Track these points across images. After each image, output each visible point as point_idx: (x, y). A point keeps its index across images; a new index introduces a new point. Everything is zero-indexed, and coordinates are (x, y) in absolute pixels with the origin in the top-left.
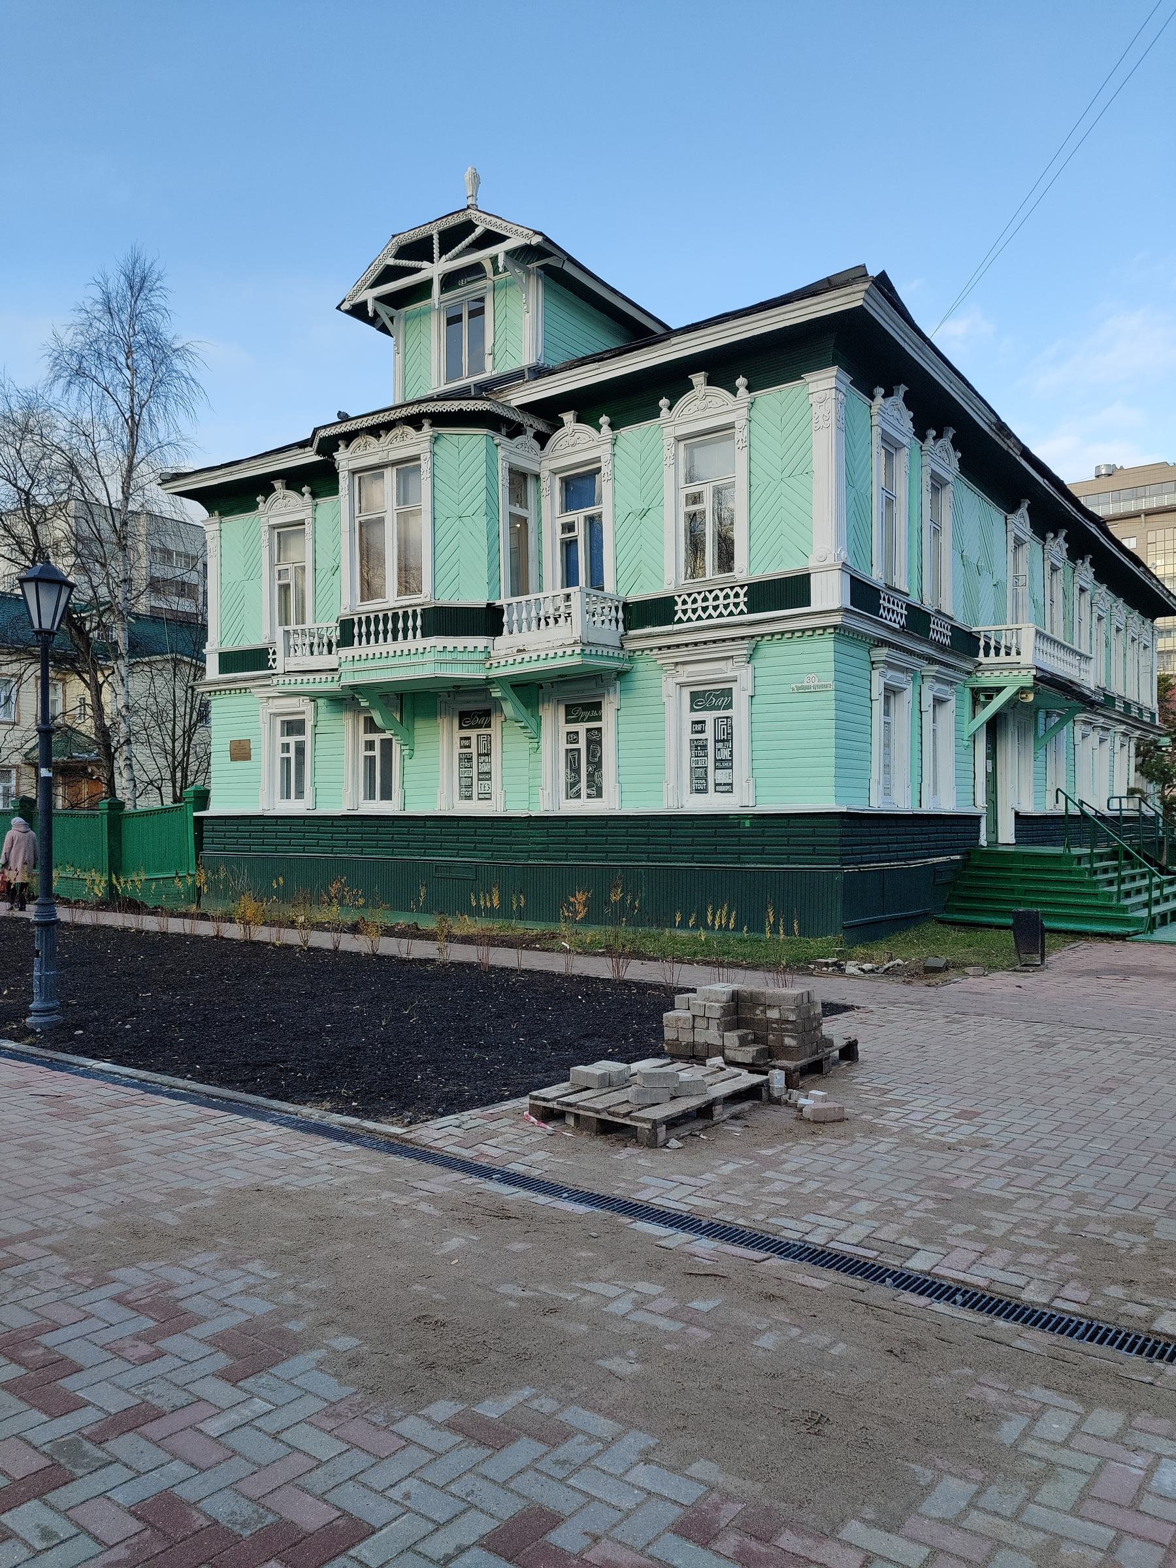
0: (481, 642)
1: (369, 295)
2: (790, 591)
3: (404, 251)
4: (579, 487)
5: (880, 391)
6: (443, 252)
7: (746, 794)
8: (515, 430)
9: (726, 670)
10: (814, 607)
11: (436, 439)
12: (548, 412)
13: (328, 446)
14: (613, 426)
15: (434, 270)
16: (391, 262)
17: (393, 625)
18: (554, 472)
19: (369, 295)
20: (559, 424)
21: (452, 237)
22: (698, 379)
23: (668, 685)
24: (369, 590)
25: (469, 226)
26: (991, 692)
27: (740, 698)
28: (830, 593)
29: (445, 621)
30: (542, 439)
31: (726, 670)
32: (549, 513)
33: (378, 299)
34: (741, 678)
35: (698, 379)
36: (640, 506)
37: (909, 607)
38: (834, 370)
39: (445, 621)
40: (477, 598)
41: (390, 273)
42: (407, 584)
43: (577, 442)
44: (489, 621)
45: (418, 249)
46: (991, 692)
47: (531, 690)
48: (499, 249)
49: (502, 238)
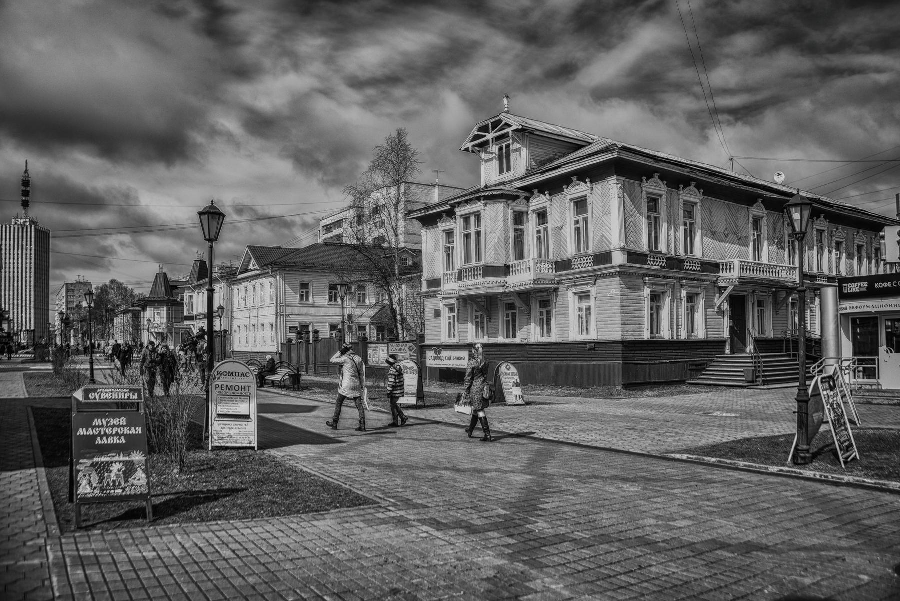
0: (503, 279)
1: (470, 145)
2: (603, 258)
3: (480, 130)
4: (542, 216)
5: (644, 178)
6: (493, 129)
7: (594, 335)
8: (515, 198)
9: (587, 288)
10: (614, 264)
11: (485, 205)
12: (529, 190)
13: (453, 206)
14: (550, 195)
15: (490, 136)
16: (476, 133)
17: (473, 272)
18: (534, 211)
19: (470, 145)
20: (533, 194)
21: (495, 125)
22: (574, 179)
23: (570, 293)
24: (468, 259)
25: (500, 121)
26: (725, 288)
27: (592, 298)
28: (619, 259)
29: (490, 271)
30: (528, 199)
31: (587, 288)
32: (531, 227)
33: (473, 146)
34: (593, 290)
35: (574, 179)
36: (560, 225)
37: (668, 259)
38: (615, 177)
39: (490, 271)
40: (501, 262)
41: (476, 138)
42: (479, 258)
43: (539, 201)
44: (506, 270)
45: (485, 129)
46: (725, 288)
47: (525, 296)
48: (509, 130)
49: (510, 126)
